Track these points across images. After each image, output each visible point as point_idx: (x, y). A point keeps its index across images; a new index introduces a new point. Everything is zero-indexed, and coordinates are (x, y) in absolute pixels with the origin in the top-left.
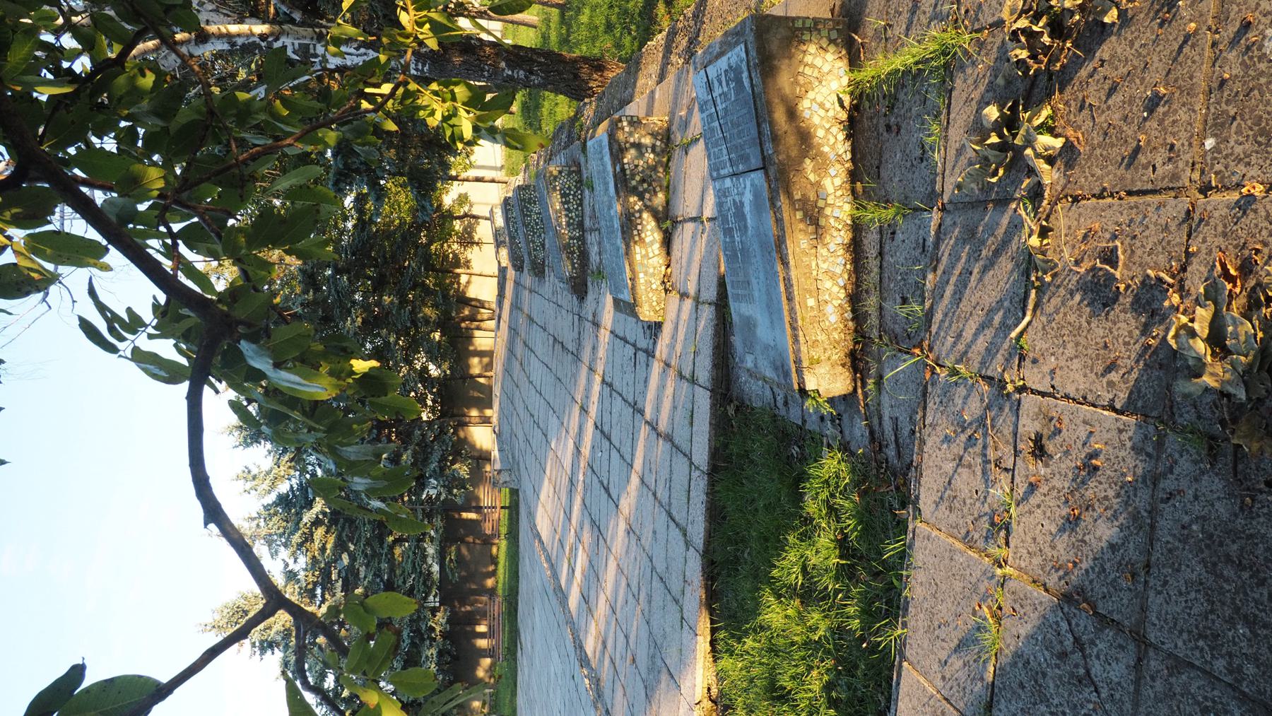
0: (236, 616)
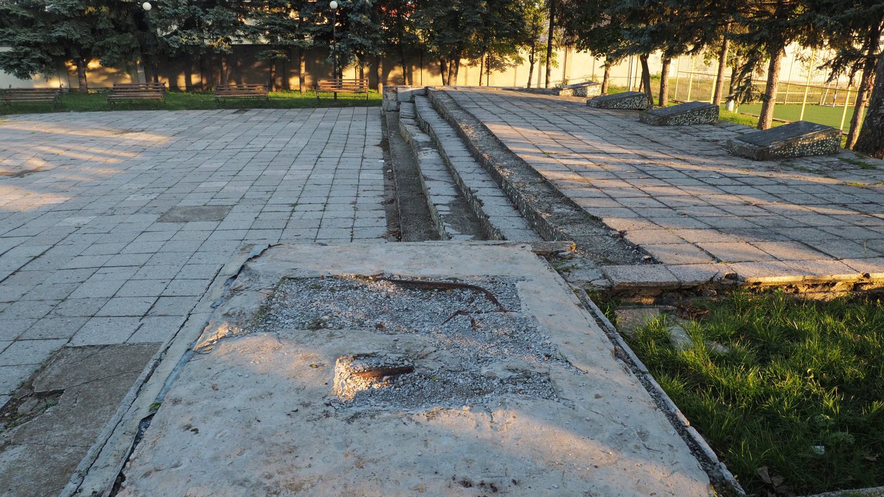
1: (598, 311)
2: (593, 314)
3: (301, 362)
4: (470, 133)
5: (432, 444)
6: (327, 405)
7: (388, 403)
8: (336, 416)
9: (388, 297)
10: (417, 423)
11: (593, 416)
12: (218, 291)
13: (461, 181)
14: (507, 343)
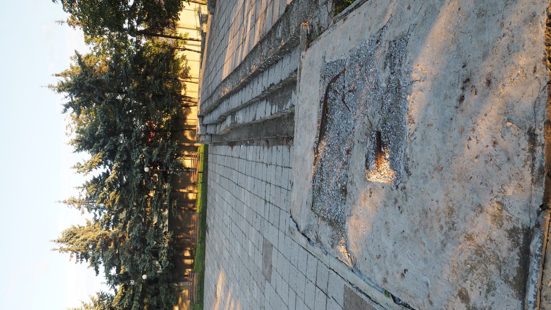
0: (70, 236)
1: (349, 8)
2: (351, 11)
3: (367, 203)
4: (227, 90)
5: (431, 121)
6: (397, 187)
7: (400, 149)
8: (405, 182)
9: (329, 146)
10: (416, 130)
11: (422, 12)
12: (316, 250)
13: (257, 97)
14: (366, 69)
